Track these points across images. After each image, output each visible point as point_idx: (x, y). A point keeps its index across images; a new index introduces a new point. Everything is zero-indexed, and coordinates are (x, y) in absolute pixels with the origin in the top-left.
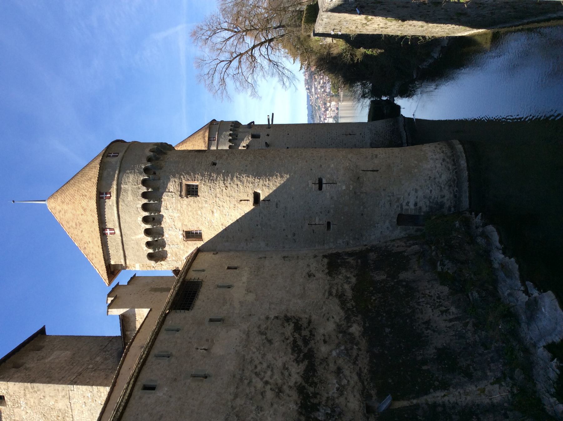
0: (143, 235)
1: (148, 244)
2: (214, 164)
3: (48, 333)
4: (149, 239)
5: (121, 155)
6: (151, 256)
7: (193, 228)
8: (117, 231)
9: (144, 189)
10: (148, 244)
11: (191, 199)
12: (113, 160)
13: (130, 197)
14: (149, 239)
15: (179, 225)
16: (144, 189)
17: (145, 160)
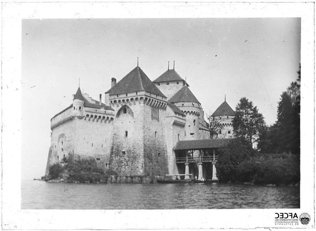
9: (229, 124)
16: (229, 124)
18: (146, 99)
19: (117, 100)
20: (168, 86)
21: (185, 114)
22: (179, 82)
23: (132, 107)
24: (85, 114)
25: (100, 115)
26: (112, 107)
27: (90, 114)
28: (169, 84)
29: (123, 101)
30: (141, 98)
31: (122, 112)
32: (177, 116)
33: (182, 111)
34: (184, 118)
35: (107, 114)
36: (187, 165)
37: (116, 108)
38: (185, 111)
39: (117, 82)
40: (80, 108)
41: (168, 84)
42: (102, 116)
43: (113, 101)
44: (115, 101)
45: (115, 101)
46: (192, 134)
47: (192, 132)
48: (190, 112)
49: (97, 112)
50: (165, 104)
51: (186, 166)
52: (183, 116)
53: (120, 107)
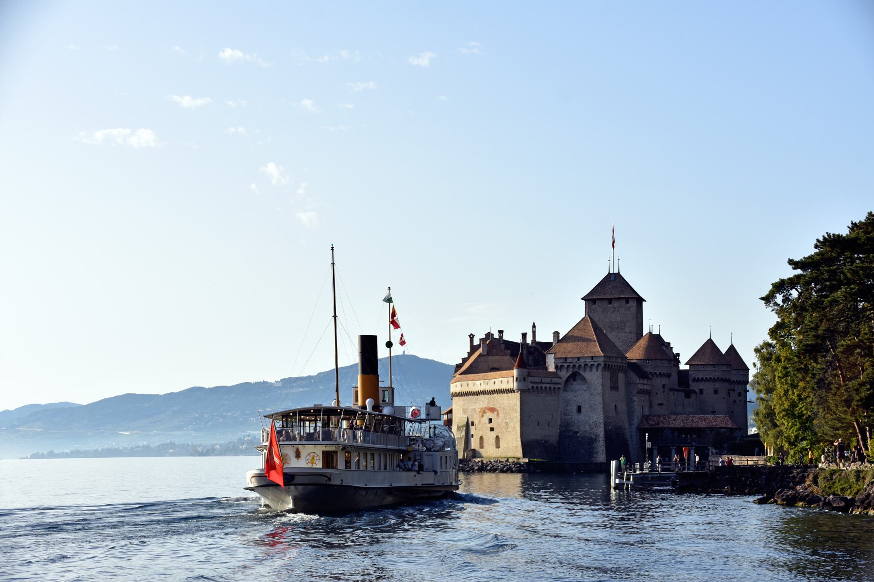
0: (701, 376)
1: (698, 378)
2: (724, 398)
3: (643, 302)
4: (700, 379)
5: (727, 369)
6: (694, 378)
7: (704, 392)
8: (703, 369)
9: (716, 378)
10: (698, 378)
11: (713, 392)
12: (725, 368)
13: (714, 374)
14: (700, 379)
15: (705, 388)
16: (716, 378)
17: (725, 377)
18: (605, 365)
19: (566, 365)
20: (610, 306)
21: (650, 376)
22: (630, 300)
23: (587, 375)
24: (530, 385)
25: (546, 385)
26: (559, 372)
27: (535, 386)
28: (612, 303)
29: (574, 366)
30: (599, 364)
31: (571, 380)
32: (641, 381)
33: (647, 372)
34: (650, 382)
35: (553, 384)
36: (655, 449)
37: (565, 374)
38: (651, 373)
39: (561, 337)
40: (524, 380)
41: (610, 303)
42: (548, 386)
43: (559, 365)
44: (562, 366)
45: (562, 366)
46: (660, 405)
47: (660, 402)
48: (658, 373)
49: (543, 381)
50: (625, 367)
51: (654, 450)
52: (648, 378)
53: (570, 373)
